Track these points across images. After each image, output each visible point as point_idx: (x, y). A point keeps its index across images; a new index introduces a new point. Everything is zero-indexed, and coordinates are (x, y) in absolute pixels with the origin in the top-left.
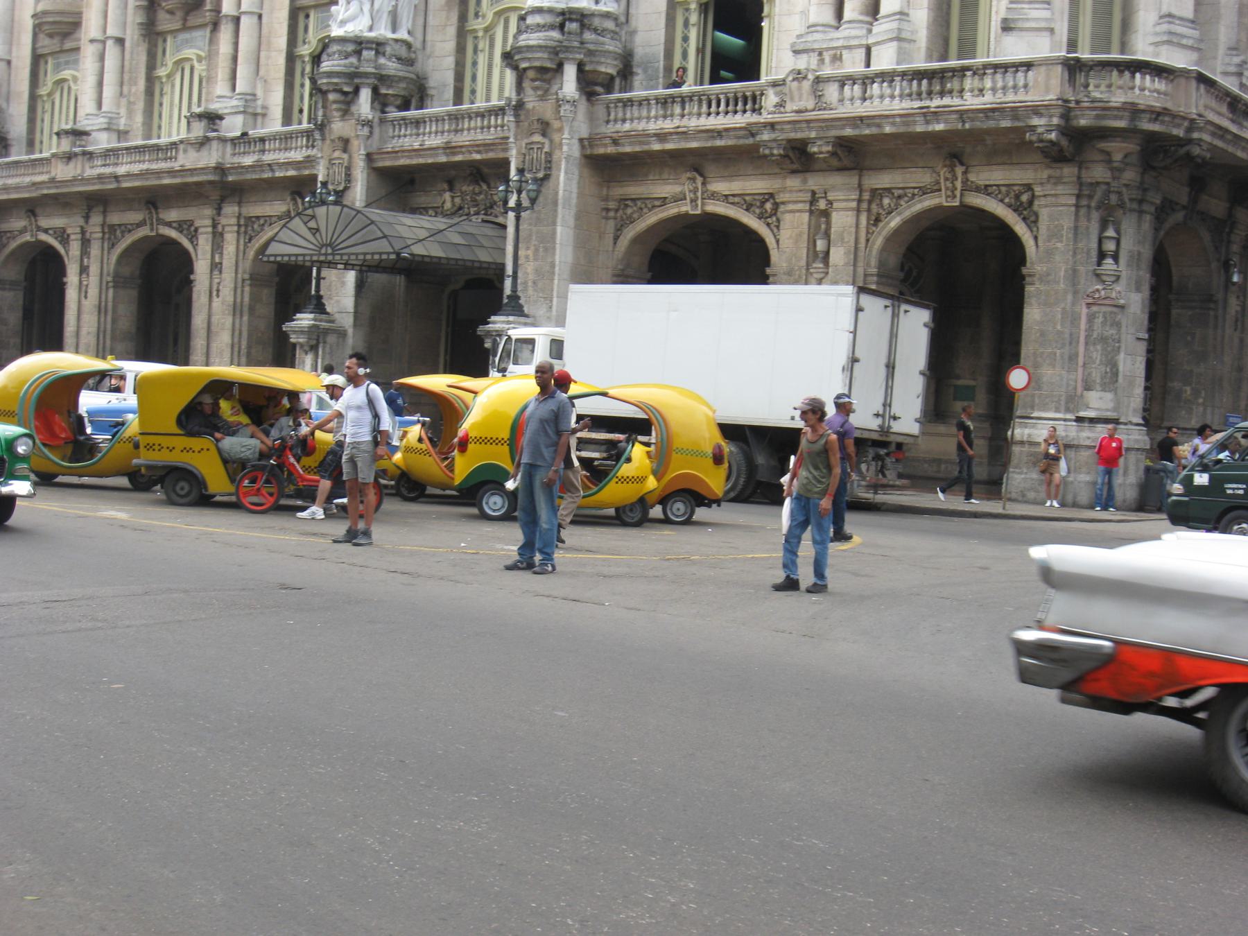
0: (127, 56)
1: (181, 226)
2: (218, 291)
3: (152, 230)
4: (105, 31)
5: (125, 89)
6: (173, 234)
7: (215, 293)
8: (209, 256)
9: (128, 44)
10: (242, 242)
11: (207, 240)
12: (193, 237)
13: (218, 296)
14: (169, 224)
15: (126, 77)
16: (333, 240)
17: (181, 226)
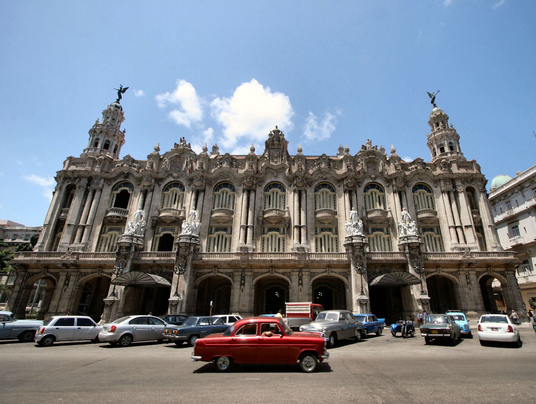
0: (254, 230)
1: (284, 274)
2: (301, 290)
3: (272, 274)
4: (247, 224)
5: (254, 238)
6: (281, 275)
7: (299, 291)
8: (298, 281)
9: (255, 227)
10: (309, 278)
11: (296, 277)
12: (289, 277)
13: (301, 291)
14: (279, 273)
15: (254, 236)
16: (137, 278)
17: (284, 274)
